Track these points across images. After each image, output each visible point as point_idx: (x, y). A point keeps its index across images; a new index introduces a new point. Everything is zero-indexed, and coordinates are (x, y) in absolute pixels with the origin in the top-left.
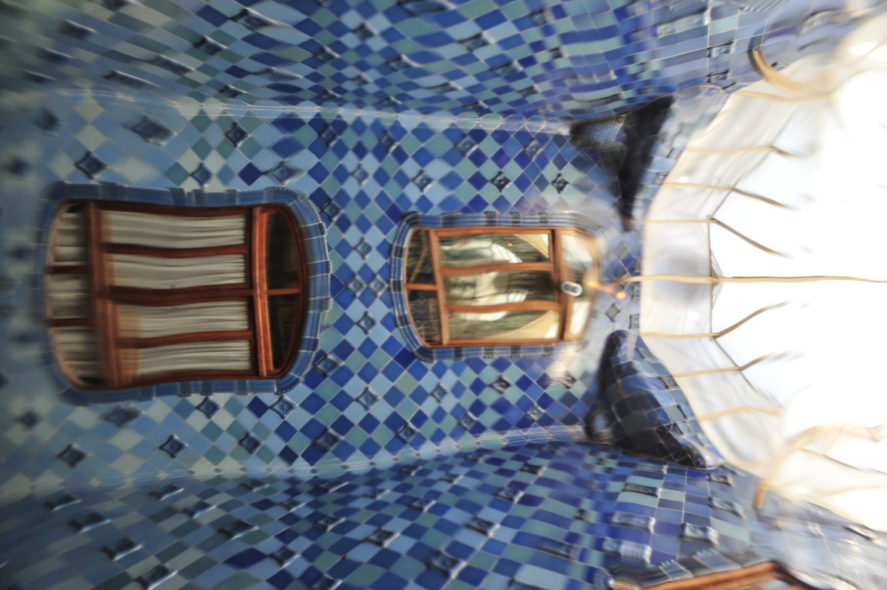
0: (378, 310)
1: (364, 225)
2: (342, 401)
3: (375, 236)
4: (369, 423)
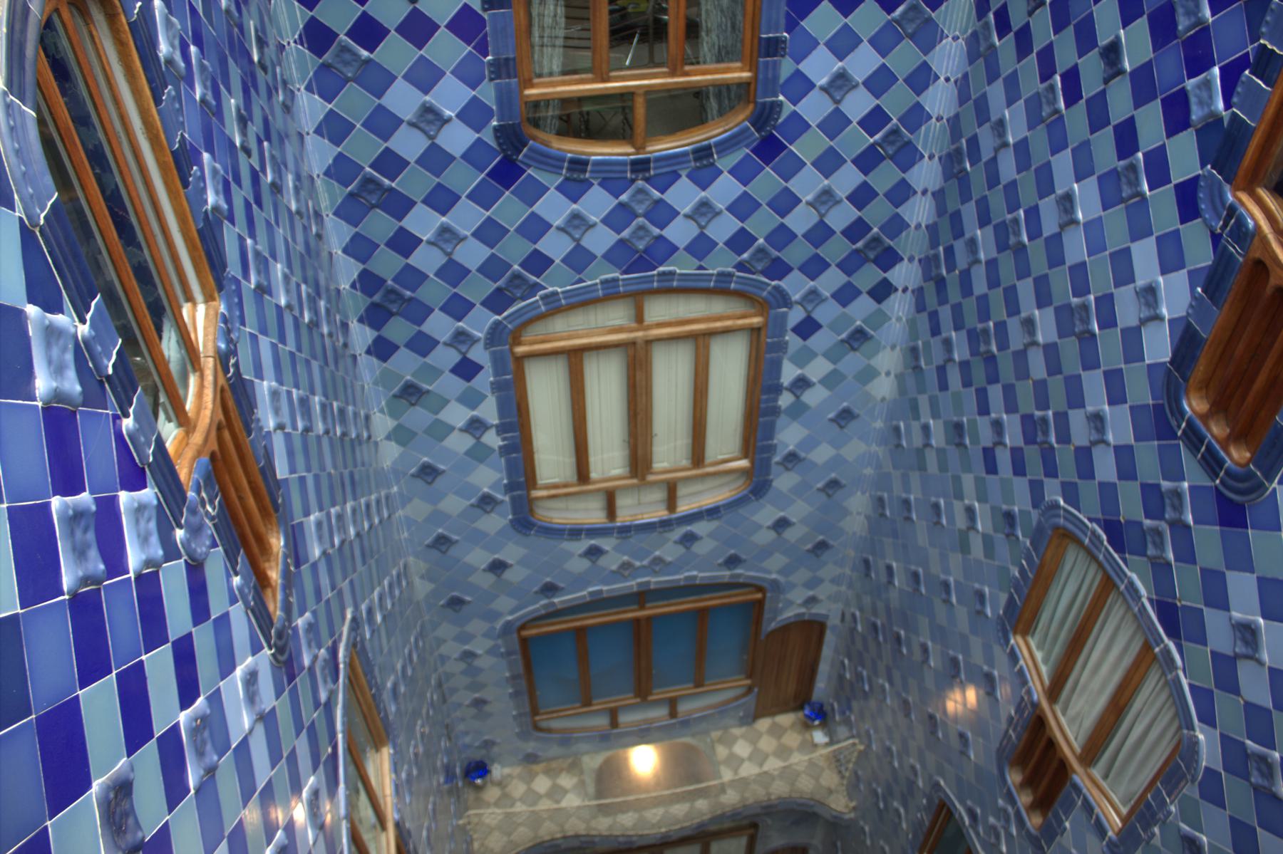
0: (683, 195)
1: (535, 227)
2: (820, 233)
3: (554, 207)
4: (861, 196)
